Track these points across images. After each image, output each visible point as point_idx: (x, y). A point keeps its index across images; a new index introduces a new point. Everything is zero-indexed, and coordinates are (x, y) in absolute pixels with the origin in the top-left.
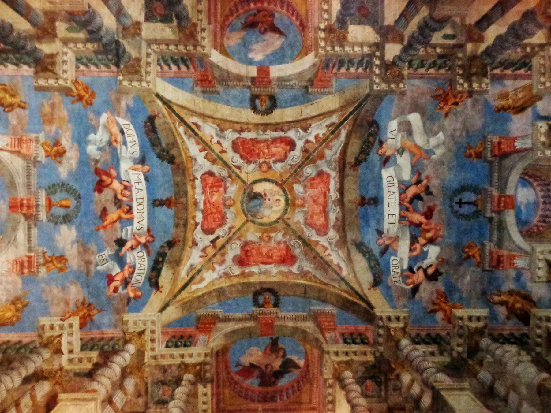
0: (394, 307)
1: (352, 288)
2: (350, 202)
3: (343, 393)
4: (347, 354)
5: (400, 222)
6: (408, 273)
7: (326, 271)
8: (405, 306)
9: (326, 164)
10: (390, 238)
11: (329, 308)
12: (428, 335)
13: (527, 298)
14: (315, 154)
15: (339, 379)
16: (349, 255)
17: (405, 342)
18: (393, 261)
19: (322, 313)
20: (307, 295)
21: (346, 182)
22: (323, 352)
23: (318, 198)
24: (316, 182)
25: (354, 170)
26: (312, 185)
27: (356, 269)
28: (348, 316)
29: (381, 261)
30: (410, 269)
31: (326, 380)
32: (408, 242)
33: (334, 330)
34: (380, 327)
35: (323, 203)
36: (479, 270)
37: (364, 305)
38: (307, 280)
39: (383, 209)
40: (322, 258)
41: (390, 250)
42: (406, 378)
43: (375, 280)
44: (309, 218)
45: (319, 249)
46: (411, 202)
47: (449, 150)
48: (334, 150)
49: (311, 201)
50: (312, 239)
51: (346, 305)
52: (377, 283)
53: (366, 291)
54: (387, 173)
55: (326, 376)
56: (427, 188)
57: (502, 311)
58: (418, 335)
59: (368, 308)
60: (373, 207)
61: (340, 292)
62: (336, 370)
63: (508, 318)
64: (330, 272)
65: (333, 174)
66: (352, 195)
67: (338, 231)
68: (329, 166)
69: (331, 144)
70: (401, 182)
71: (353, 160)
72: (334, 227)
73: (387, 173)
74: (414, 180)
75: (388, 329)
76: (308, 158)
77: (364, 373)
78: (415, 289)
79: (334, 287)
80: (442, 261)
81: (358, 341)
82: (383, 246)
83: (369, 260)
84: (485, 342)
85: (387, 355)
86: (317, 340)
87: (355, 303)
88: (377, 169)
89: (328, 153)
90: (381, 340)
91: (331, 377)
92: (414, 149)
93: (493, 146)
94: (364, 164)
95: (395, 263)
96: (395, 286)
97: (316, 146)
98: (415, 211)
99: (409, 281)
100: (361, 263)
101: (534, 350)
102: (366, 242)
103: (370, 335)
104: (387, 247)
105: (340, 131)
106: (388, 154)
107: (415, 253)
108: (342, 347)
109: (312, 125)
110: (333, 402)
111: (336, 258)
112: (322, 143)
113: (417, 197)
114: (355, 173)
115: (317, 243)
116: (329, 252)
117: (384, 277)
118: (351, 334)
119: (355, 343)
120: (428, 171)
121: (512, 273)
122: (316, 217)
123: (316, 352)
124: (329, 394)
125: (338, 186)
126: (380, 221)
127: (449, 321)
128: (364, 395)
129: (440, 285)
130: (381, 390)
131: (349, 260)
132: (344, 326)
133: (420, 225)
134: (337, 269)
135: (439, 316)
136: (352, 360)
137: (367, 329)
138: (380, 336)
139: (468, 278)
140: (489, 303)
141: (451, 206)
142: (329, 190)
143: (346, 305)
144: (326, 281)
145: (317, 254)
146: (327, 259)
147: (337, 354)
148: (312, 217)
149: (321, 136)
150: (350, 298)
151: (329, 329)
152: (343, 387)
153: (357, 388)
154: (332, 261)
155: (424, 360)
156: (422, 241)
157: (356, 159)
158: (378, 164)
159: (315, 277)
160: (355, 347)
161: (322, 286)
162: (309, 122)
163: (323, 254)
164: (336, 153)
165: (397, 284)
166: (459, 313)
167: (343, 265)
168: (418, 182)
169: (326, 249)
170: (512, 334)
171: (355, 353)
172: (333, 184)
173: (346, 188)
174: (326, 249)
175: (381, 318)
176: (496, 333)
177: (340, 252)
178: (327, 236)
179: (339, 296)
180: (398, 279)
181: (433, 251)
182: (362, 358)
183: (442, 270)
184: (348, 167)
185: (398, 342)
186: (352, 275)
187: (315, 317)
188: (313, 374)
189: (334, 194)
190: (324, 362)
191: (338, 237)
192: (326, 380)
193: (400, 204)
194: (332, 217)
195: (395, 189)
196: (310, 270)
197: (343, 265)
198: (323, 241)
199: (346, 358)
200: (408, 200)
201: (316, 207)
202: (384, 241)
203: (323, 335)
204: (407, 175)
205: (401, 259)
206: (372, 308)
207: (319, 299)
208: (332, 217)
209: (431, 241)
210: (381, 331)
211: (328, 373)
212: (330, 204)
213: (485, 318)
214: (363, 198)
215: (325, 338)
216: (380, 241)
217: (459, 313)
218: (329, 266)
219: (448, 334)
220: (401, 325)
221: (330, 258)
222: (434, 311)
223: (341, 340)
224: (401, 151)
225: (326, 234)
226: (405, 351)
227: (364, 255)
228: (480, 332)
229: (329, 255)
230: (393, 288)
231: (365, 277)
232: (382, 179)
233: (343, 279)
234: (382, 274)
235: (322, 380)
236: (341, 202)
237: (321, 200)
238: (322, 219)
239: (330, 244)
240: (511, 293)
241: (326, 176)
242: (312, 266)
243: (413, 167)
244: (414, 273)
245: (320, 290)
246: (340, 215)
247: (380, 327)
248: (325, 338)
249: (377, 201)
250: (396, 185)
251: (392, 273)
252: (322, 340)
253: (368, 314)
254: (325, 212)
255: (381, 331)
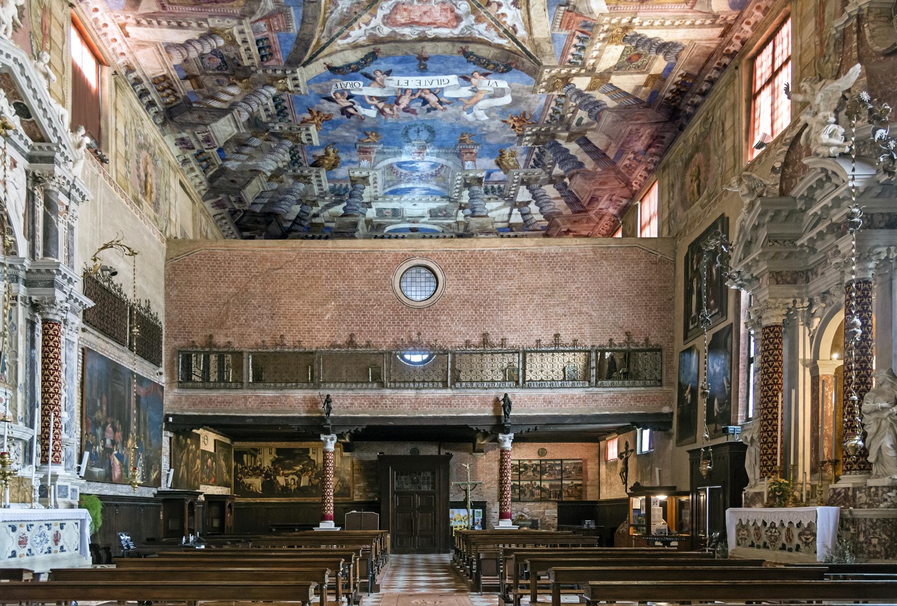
0: (308, 83)
1: (323, 48)
2: (423, 48)
3: (197, 38)
4: (245, 41)
5: (402, 89)
6: (346, 94)
7: (340, 23)
8: (311, 91)
9: (469, 24)
10: (382, 81)
11: (295, 27)
12: (286, 108)
13: (334, 166)
14: (483, 13)
15: (212, 33)
16: (362, 46)
17: (273, 91)
18: (359, 84)
19: (288, 19)
20: (307, 4)
21: (446, 44)
22: (241, 18)
23: (429, 17)
24: (449, 15)
25: (459, 52)
26: (445, 10)
27: (345, 52)
28: (290, 45)
29: (358, 73)
30: (350, 97)
31: (206, 20)
32: (380, 95)
33: (270, 29)
34: (284, 71)
35: (422, 21)
36: (355, 141)
37: (306, 58)
38: (326, 4)
39: (415, 75)
40: (356, 20)
41: (370, 81)
42: (233, 90)
43: (336, 68)
44: (405, 7)
45: (366, 17)
46: (420, 97)
47: (470, 123)
48: (485, 33)
49: (425, 9)
50: (379, 11)
51: (303, 42)
52: (333, 70)
53: (322, 61)
54: (453, 79)
55: (210, 20)
56: (435, 109)
57: (321, 153)
58: (283, 100)
59: (303, 62)
60: (416, 67)
61: (317, 37)
62: (223, 31)
63: (314, 156)
64: (339, 28)
65: (456, 32)
66: (429, 49)
67: (389, 36)
68: (466, 27)
69: (492, 30)
70: (442, 90)
71: (470, 50)
72: (394, 32)
73: (453, 79)
74: (442, 99)
75: (284, 78)
76: (479, 6)
77: (228, 57)
78: (330, 99)
79: (322, 31)
80: (362, 119)
81: (263, 52)
82: (373, 75)
83: (358, 63)
84: (289, 144)
85: (255, 76)
86: (253, 13)
87: (306, 50)
88: (458, 71)
89: (482, 27)
90: (270, 72)
91: (211, 26)
92: (475, 99)
93: (468, 149)
94: (465, 60)
95: (357, 85)
96: (331, 85)
97: (493, 15)
98: (411, 101)
99: (338, 95)
100: (353, 57)
101: (290, 168)
102: (378, 61)
103: (273, 62)
104: (373, 79)
105: (505, 38)
106: (473, 80)
107: (368, 100)
108: (251, 38)
109: (518, 11)
110: (180, 26)
111: (357, 34)
112: (495, 21)
113: (425, 102)
114: (455, 52)
115: (375, 16)
116: (364, 27)
117: (339, 76)
118: (269, 47)
119: (260, 49)
120: (450, 110)
121: (355, 159)
122: (405, 14)
123: (237, 11)
124: (189, 24)
125: (442, 36)
126: (401, 73)
127: (302, 122)
128: (202, 56)
129: (337, 116)
130: (213, 70)
131: (355, 46)
132: (277, 40)
133: (398, 104)
134: (344, 34)
135: (308, 116)
136: (239, 46)
137: (278, 60)
138: (275, 71)
139: (347, 134)
140: (325, 147)
141: (415, 125)
142: (438, 27)
143: (303, 42)
144: (328, 24)
145: (360, 16)
146: (355, 25)
147: (242, 32)
148: (405, 10)
149: (504, 19)
150: (312, 47)
151: (270, 26)
152: (203, 38)
153: (208, 50)
154: (353, 29)
155: (258, 104)
156: (381, 105)
157: (472, 53)
158: (463, 72)
159: (332, 12)
160: (254, 50)
161: (321, 20)
162: (524, 8)
163: (360, 21)
164: (480, 34)
165: (334, 86)
166: (313, 129)
167: (349, 40)
168: (441, 103)
169: (367, 24)
170: (300, 158)
171: (248, 49)
172: (444, 32)
173: (439, 44)
174: (367, 24)
175: (293, 72)
176: (299, 149)
177: (365, 38)
178: (382, 26)
179: (313, 36)
180: (339, 86)
181: (372, 113)
182: (244, 56)
183: (352, 118)
184: (464, 46)
185: (272, 85)
186: (339, 48)
187: (280, 11)
188: (208, 8)
189: (432, 32)
190: (228, 19)
191: (381, 36)
192: (206, 20)
193: (419, 89)
194: (406, 31)
195: (435, 85)
196: (339, 8)
197: (349, 40)
198: (377, 21)
199: (239, 40)
200: (423, 95)
201: (418, 14)
202: (379, 77)
203: (261, 19)
204: (448, 94)
205: (361, 90)
206: (304, 65)
207: (304, 16)
208: (406, 31)
209: (381, 112)
210: (279, 72)
211: (214, 23)
212: (421, 29)
213: (312, 144)
214: (426, 59)
215: (257, 21)
216: (379, 73)
217: (313, 129)
218: (347, 27)
219: (290, 121)
220: (290, 88)
221: (357, 28)
222: (310, 112)
223: (259, 37)
224: (475, 90)
225: (384, 24)
226: (263, 91)
227: (362, 59)
228: (298, 140)
229: (360, 28)
230: (329, 83)
231: (338, 61)
232: (447, 75)
233: (332, 40)
234: (343, 74)
235: (204, 17)
236: (423, 39)
237: (426, 20)
238: (403, 21)
239: (373, 28)
240: (337, 158)
241: (455, 24)
242: (345, 10)
243: (457, 99)
244: (348, 99)
245: (315, 18)
246: (408, 39)
247: (284, 71)
248: (257, 21)
249: (423, 70)
250: (439, 86)
251: (345, 82)
252: (253, 19)
253: (294, 62)
254: (411, 23)
255: (279, 72)
